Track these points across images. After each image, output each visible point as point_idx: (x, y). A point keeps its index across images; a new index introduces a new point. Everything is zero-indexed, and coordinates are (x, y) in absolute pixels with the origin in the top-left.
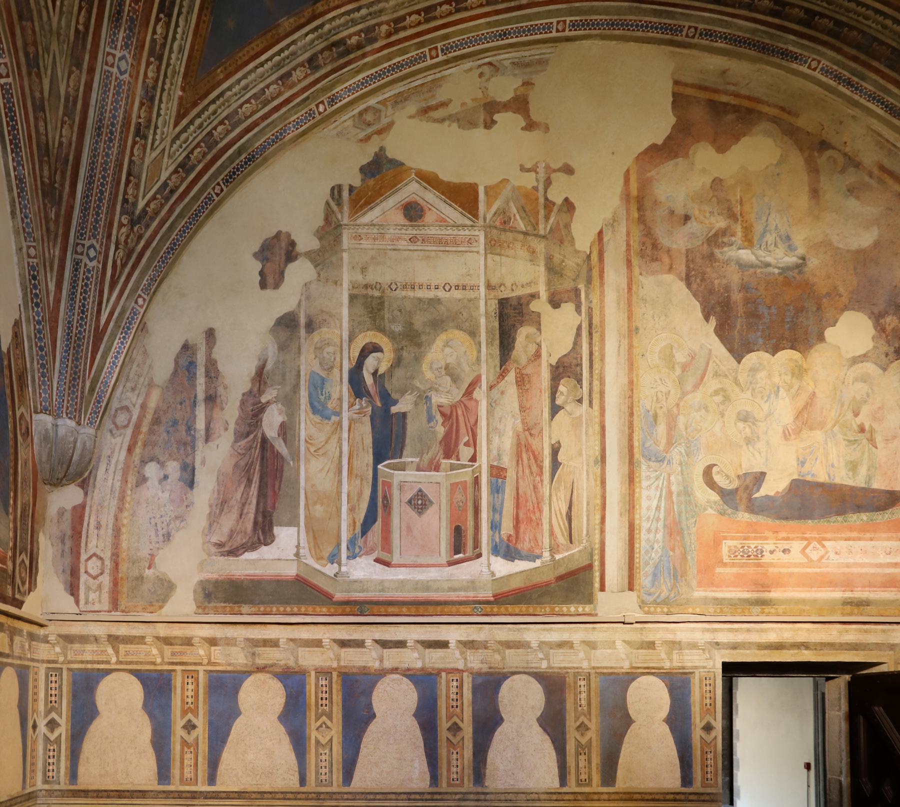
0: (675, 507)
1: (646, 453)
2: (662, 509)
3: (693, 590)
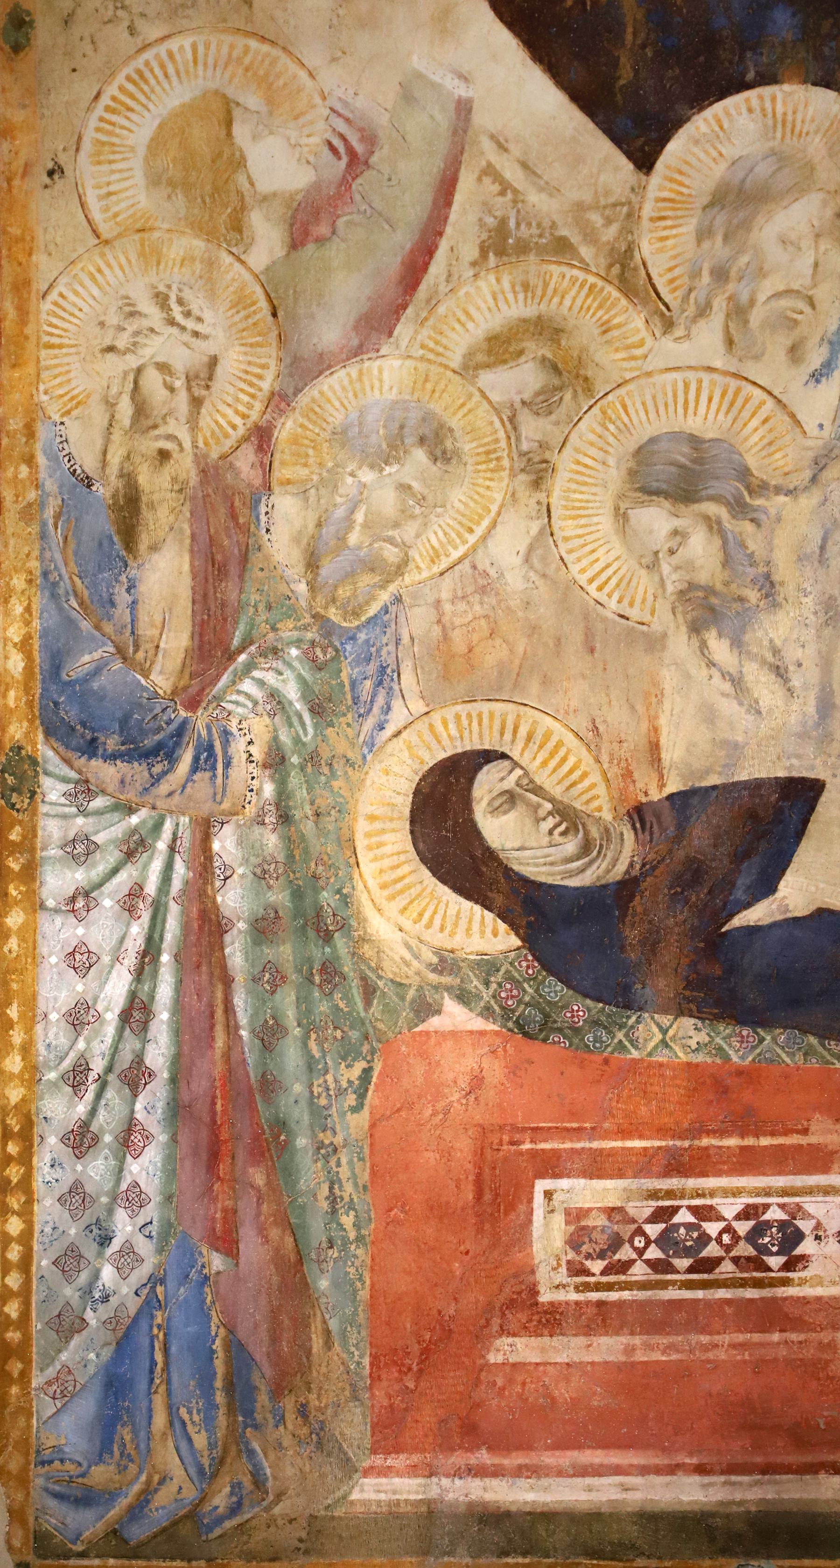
0: (240, 1000)
1: (71, 713)
2: (163, 1016)
3: (349, 1469)
